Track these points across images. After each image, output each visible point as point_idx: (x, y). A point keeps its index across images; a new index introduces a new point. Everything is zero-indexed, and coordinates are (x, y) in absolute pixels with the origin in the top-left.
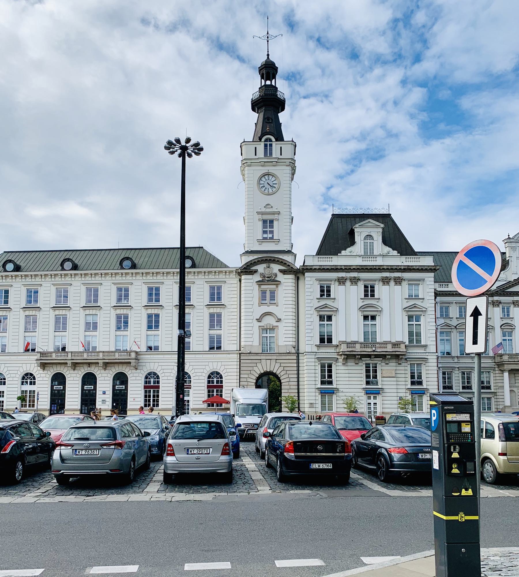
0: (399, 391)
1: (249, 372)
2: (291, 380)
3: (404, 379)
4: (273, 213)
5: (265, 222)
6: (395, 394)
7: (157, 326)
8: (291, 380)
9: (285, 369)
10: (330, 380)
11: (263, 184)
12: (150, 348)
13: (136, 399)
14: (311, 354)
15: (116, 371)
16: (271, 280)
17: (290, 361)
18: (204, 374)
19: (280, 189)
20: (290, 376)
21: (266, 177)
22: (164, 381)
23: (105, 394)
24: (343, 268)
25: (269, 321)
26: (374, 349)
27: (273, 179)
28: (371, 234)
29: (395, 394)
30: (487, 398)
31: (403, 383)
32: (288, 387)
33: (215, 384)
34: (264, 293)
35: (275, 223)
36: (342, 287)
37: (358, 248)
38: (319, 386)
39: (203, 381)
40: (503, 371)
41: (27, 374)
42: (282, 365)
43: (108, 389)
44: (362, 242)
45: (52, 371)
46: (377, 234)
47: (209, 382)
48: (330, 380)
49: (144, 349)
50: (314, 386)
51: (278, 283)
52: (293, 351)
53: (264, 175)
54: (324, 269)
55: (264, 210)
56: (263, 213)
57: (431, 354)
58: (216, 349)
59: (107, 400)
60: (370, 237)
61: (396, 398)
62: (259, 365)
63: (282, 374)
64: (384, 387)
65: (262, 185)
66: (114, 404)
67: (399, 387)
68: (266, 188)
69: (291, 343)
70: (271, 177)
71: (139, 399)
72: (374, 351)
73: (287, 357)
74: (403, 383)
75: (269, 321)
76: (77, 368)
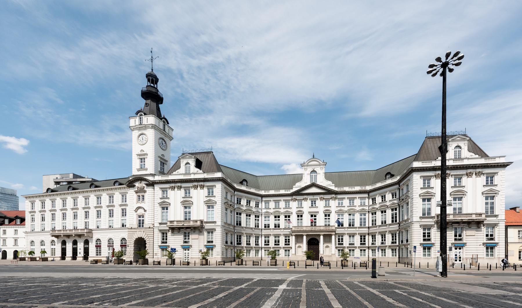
0: (200, 246)
3: (203, 240)
5: (141, 159)
6: (198, 248)
7: (125, 215)
9: (148, 236)
16: (142, 190)
17: (150, 232)
18: (119, 240)
20: (150, 239)
21: (142, 136)
24: (171, 181)
25: (141, 211)
26: (183, 224)
27: (145, 136)
29: (198, 248)
30: (352, 250)
31: (203, 242)
33: (124, 244)
34: (139, 196)
35: (146, 159)
37: (182, 170)
41: (123, 239)
43: (81, 247)
46: (192, 162)
51: (145, 192)
53: (141, 135)
54: (162, 182)
55: (140, 153)
57: (218, 226)
59: (81, 252)
60: (188, 163)
64: (192, 244)
65: (140, 140)
66: (85, 254)
67: (200, 244)
70: (144, 135)
72: (183, 225)
74: (203, 242)
75: (141, 211)
76: (81, 237)
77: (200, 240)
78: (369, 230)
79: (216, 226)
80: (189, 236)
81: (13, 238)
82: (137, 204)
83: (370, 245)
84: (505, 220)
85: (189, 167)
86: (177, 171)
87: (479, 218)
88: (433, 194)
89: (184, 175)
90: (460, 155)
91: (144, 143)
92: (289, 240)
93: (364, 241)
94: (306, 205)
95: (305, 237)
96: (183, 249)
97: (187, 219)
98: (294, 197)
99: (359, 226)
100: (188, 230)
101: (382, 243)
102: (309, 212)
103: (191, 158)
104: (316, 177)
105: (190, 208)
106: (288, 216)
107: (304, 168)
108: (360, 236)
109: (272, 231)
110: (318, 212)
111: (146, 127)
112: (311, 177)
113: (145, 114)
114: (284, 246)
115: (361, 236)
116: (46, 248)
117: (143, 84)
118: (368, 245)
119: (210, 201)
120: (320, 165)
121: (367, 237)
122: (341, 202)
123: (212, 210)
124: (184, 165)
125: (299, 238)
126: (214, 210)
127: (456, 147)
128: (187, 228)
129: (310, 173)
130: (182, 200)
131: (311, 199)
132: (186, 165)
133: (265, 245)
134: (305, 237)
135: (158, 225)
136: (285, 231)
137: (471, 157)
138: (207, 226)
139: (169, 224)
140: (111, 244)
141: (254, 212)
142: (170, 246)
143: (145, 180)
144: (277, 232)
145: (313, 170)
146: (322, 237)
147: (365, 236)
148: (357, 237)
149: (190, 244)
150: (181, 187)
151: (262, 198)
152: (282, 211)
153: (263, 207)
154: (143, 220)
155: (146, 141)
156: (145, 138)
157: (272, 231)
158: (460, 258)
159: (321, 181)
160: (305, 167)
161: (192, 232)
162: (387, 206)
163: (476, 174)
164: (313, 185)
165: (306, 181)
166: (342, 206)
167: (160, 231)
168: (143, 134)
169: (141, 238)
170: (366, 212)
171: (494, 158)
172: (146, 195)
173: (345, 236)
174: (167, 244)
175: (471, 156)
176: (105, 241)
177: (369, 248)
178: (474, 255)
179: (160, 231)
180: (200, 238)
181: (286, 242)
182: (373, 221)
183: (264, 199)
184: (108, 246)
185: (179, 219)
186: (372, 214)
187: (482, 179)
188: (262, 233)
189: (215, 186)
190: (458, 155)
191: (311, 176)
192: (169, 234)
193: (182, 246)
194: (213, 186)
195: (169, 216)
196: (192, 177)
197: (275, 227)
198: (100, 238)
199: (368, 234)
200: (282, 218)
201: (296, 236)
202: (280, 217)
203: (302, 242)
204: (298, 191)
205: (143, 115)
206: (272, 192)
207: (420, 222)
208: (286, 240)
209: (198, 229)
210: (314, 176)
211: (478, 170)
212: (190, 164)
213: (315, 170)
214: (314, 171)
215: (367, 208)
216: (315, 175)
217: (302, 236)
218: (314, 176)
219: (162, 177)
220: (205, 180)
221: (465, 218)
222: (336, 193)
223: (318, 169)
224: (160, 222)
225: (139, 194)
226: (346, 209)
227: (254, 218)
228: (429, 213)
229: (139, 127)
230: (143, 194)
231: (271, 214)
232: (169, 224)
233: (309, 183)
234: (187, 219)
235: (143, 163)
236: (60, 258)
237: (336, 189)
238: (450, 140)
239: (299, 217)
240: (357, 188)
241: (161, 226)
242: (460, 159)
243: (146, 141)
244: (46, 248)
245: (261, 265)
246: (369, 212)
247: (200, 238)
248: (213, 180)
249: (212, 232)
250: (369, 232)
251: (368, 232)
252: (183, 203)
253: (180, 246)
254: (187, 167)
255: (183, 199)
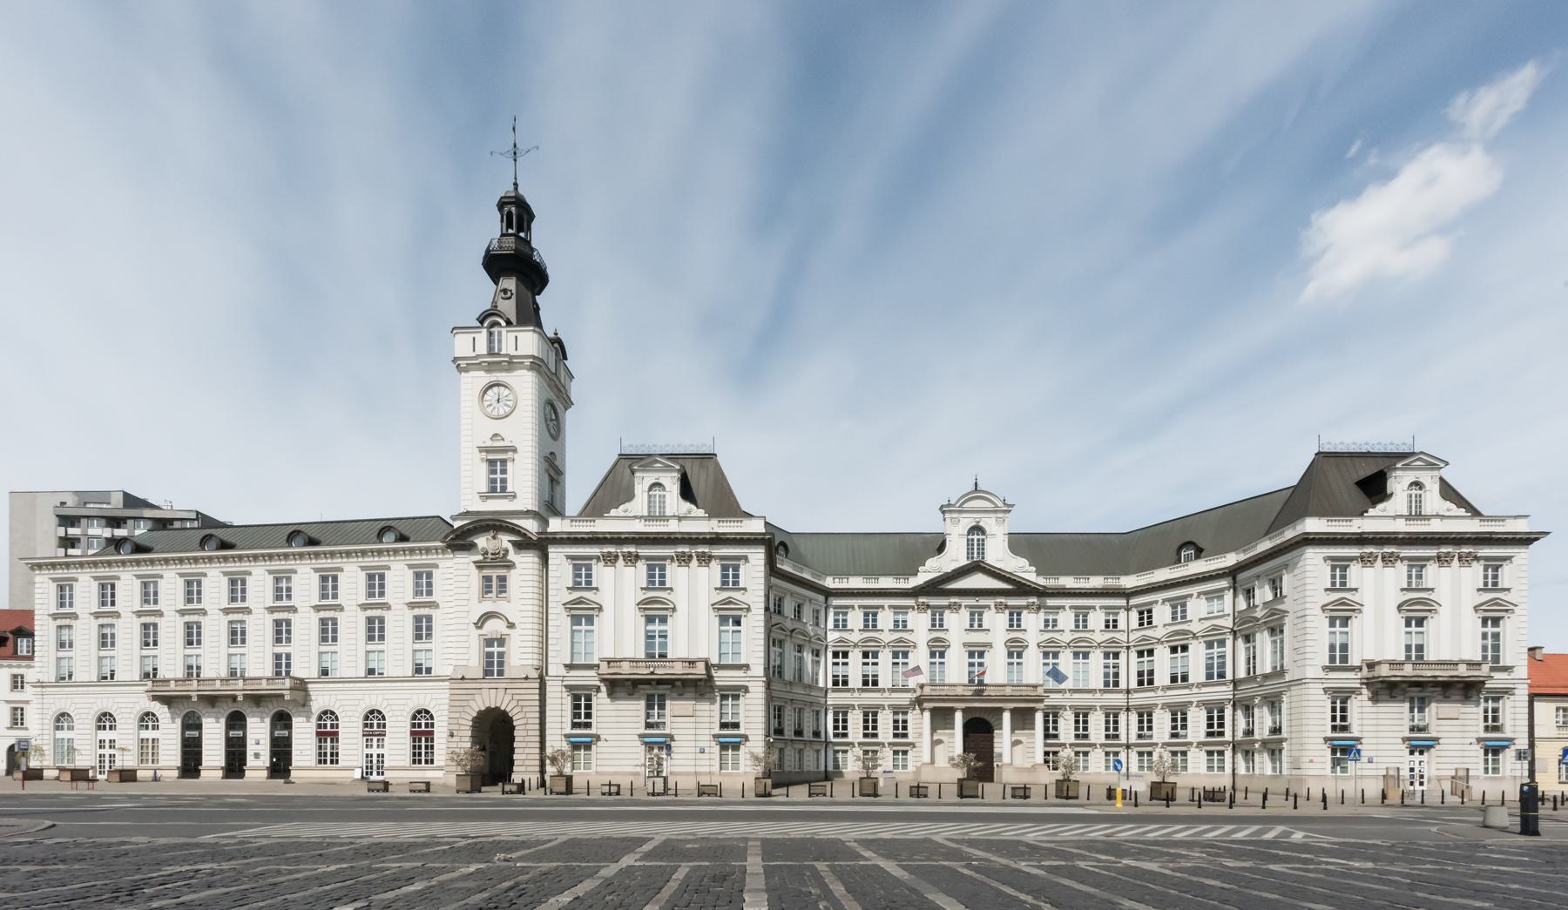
1: (461, 709)
2: (530, 721)
3: (707, 719)
4: (505, 450)
5: (492, 463)
8: (530, 721)
10: (589, 720)
11: (490, 401)
12: (371, 671)
13: (304, 752)
14: (556, 678)
15: (274, 708)
19: (517, 409)
21: (495, 389)
22: (346, 725)
23: (258, 744)
26: (652, 669)
28: (660, 481)
29: (693, 744)
31: (707, 725)
32: (524, 733)
34: (487, 579)
35: (509, 465)
36: (610, 570)
37: (639, 505)
38: (568, 730)
39: (404, 724)
40: (922, 710)
42: (516, 697)
44: (646, 495)
45: (271, 707)
46: (671, 483)
47: (413, 725)
48: (589, 720)
49: (315, 673)
50: (559, 732)
52: (535, 674)
55: (489, 443)
56: (488, 450)
57: (754, 679)
58: (498, 675)
61: (693, 750)
62: (478, 698)
63: (515, 711)
65: (488, 403)
67: (698, 732)
68: (494, 408)
69: (530, 662)
70: (502, 388)
71: (309, 752)
72: (652, 673)
73: (525, 685)
74: (707, 725)
77: (698, 719)
78: (1128, 699)
79: (748, 679)
80: (662, 707)
81: (8, 702)
82: (480, 602)
83: (1133, 739)
84: (1529, 681)
85: (660, 496)
86: (622, 507)
87: (1476, 673)
88: (1358, 607)
89: (646, 520)
90: (1420, 507)
91: (502, 412)
92: (905, 721)
93: (1116, 729)
94: (957, 622)
95: (959, 717)
96: (643, 746)
97: (656, 655)
98: (921, 600)
99: (1102, 687)
100: (662, 689)
101: (1174, 735)
102: (965, 645)
103: (667, 469)
104: (981, 544)
105: (663, 620)
106: (873, 652)
107: (952, 518)
108: (862, 715)
109: (1160, 693)
110: (990, 645)
111: (511, 364)
112: (970, 543)
113: (509, 323)
114: (1073, 740)
115: (866, 714)
116: (164, 737)
117: (489, 230)
118: (1233, 736)
119: (730, 603)
120: (996, 512)
121: (1122, 718)
122: (1051, 617)
123: (586, 631)
124: (646, 488)
125: (941, 717)
126: (592, 631)
127: (1411, 484)
128: (660, 682)
129: (966, 533)
130: (642, 596)
131: (971, 607)
132: (650, 489)
133: (836, 735)
134: (959, 717)
135: (563, 672)
136: (894, 695)
137: (1447, 514)
138: (722, 678)
139: (604, 666)
140: (375, 728)
141: (1159, 640)
142: (601, 736)
143: (513, 530)
144: (871, 698)
145: (974, 524)
146: (1007, 716)
147: (1116, 716)
148: (1096, 718)
149: (667, 731)
150: (711, 557)
151: (826, 600)
152: (887, 637)
153: (830, 624)
154: (501, 655)
155: (509, 406)
156: (508, 403)
157: (886, 695)
158: (1422, 777)
159: (998, 554)
160: (954, 515)
161: (675, 695)
162: (1194, 634)
163: (1460, 559)
164: (976, 567)
165: (955, 556)
166: (1056, 629)
167: (569, 688)
168: (498, 385)
169: (497, 709)
170: (1122, 647)
171: (1502, 519)
172: (513, 577)
173: (854, 711)
174: (593, 731)
175: (1448, 510)
176: (353, 719)
177: (1128, 747)
178: (1391, 768)
179: (569, 688)
180: (698, 713)
181: (896, 728)
182: (1140, 674)
183: (836, 602)
184: (364, 735)
185: (630, 654)
186: (1140, 654)
187: (1474, 574)
188: (1128, 702)
189: (746, 558)
190: (1416, 507)
191: (968, 540)
192: (601, 701)
193: (641, 736)
194: (738, 558)
195: (596, 644)
196: (673, 527)
197: (865, 683)
198: (431, 705)
199: (1128, 710)
200: (885, 657)
201: (934, 711)
202: (850, 654)
203: (950, 725)
204: (933, 584)
205: (503, 324)
206: (856, 583)
207: (1323, 681)
208: (896, 721)
209: (698, 686)
210: (975, 541)
211: (1465, 550)
212: (664, 489)
213: (981, 524)
214: (977, 529)
215: (1122, 637)
216: (978, 540)
217: (952, 710)
218: (975, 541)
219: (574, 523)
220: (717, 540)
221: (1443, 674)
222: (1043, 593)
223: (988, 523)
224: (568, 662)
225: (486, 572)
226: (1067, 637)
227: (860, 660)
228: (1344, 659)
229: (489, 363)
230: (502, 572)
231: (856, 646)
232: (604, 668)
233: (963, 561)
234: (656, 655)
235: (499, 476)
236: (221, 771)
237: (1041, 581)
238: (1399, 465)
239: (838, 657)
240: (1096, 582)
241: (573, 673)
242: (1419, 516)
243: (509, 406)
244: (164, 737)
245: (831, 796)
246: (1128, 648)
247: (698, 713)
248: (691, 539)
249: (736, 697)
250: (1128, 702)
251: (1126, 704)
252: (644, 605)
253: (637, 738)
254: (655, 496)
255: (645, 594)
